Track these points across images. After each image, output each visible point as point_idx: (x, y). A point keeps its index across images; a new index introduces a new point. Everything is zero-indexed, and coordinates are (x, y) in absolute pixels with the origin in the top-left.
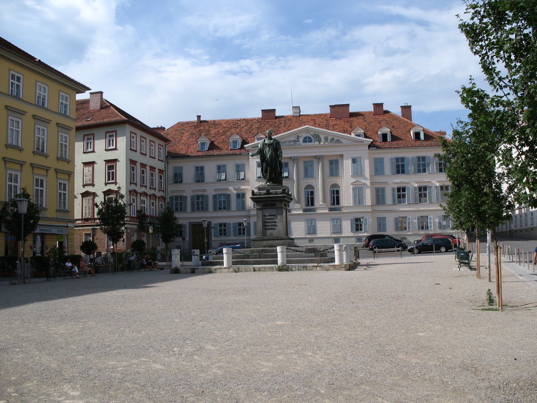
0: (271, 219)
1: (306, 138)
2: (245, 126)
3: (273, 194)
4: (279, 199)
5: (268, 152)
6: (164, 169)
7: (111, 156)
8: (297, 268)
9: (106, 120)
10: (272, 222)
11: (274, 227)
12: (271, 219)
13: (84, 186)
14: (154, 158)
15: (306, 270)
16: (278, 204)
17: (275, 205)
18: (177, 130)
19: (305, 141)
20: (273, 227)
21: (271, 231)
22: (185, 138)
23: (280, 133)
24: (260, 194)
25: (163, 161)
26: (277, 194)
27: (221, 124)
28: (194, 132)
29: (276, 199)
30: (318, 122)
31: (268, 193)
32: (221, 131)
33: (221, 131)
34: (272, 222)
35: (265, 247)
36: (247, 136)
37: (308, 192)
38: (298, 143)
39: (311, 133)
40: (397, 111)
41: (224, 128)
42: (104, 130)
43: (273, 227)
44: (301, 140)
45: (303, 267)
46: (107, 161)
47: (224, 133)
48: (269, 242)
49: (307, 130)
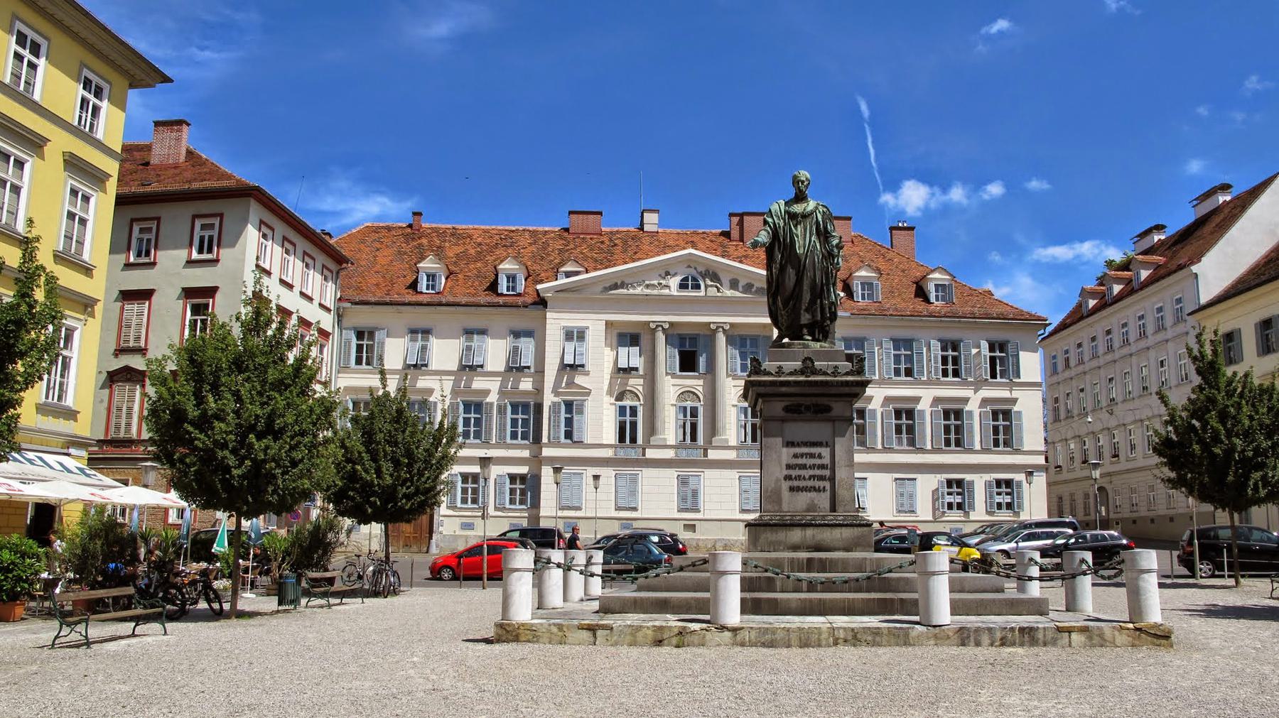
0: (812, 456)
1: (686, 279)
2: (530, 244)
3: (825, 374)
4: (846, 390)
5: (804, 240)
6: (330, 330)
8: (998, 635)
9: (196, 185)
10: (813, 467)
11: (821, 484)
12: (812, 456)
13: (120, 351)
14: (310, 299)
15: (1034, 642)
16: (838, 408)
17: (828, 409)
18: (363, 241)
19: (683, 286)
20: (817, 484)
21: (813, 494)
22: (383, 260)
23: (615, 265)
24: (780, 371)
25: (328, 310)
26: (835, 374)
27: (470, 237)
29: (834, 391)
30: (700, 245)
31: (808, 367)
32: (472, 252)
33: (472, 252)
34: (813, 467)
35: (795, 548)
36: (536, 267)
37: (685, 408)
38: (666, 291)
39: (700, 269)
41: (480, 244)
42: (184, 212)
43: (817, 484)
44: (674, 282)
45: (1022, 630)
46: (189, 293)
47: (479, 257)
48: (810, 532)
49: (690, 261)
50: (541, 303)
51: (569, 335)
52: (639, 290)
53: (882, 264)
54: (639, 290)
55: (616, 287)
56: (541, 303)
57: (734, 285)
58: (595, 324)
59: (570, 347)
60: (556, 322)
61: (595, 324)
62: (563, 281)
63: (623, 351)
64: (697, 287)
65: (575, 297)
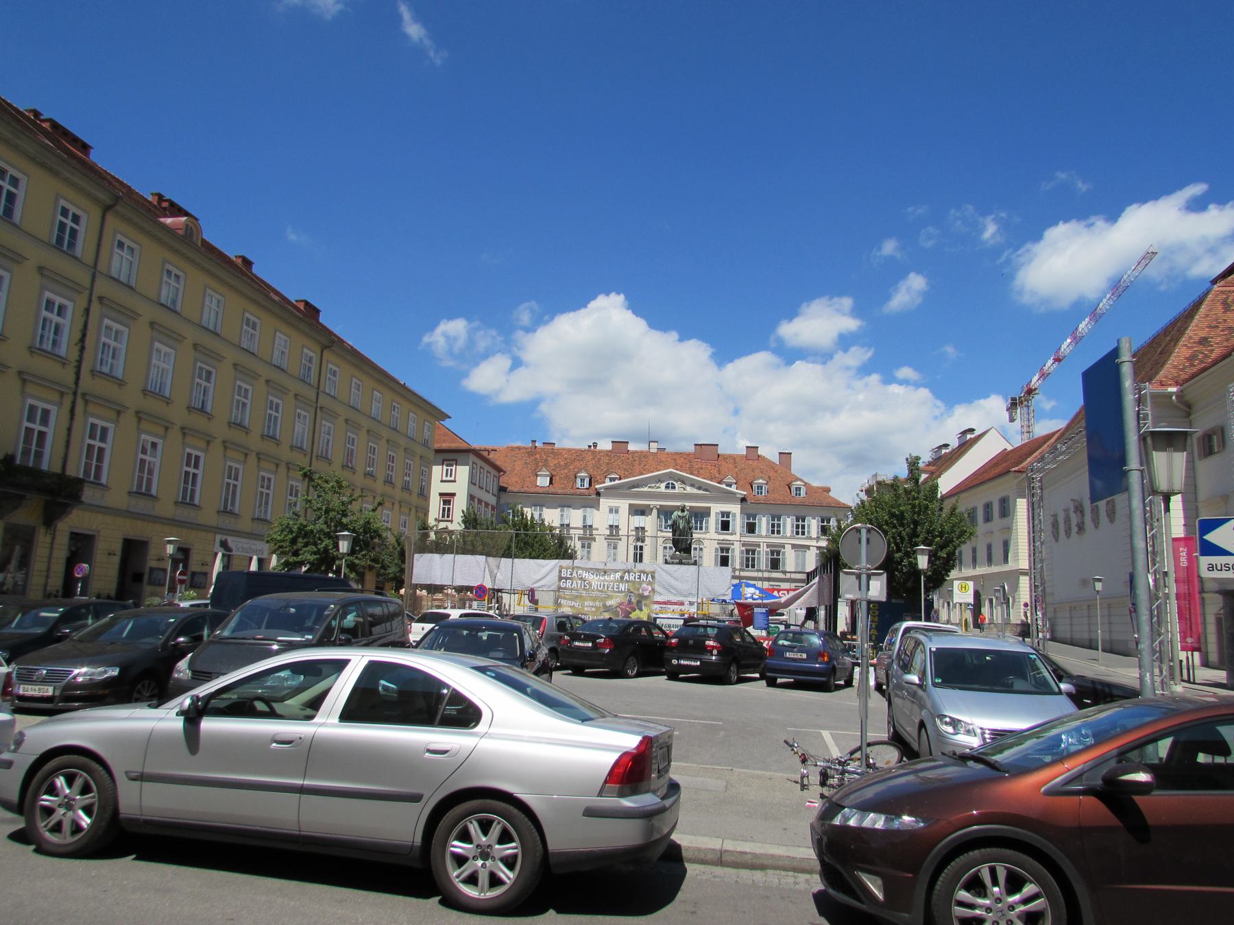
7: (448, 488)
19: (667, 487)
28: (529, 461)
40: (775, 459)
44: (663, 485)
50: (598, 494)
51: (611, 511)
52: (646, 489)
53: (772, 474)
54: (646, 489)
55: (634, 487)
56: (598, 494)
57: (692, 485)
58: (624, 505)
59: (611, 516)
60: (605, 503)
61: (624, 505)
62: (608, 483)
63: (637, 518)
64: (674, 487)
65: (613, 492)
